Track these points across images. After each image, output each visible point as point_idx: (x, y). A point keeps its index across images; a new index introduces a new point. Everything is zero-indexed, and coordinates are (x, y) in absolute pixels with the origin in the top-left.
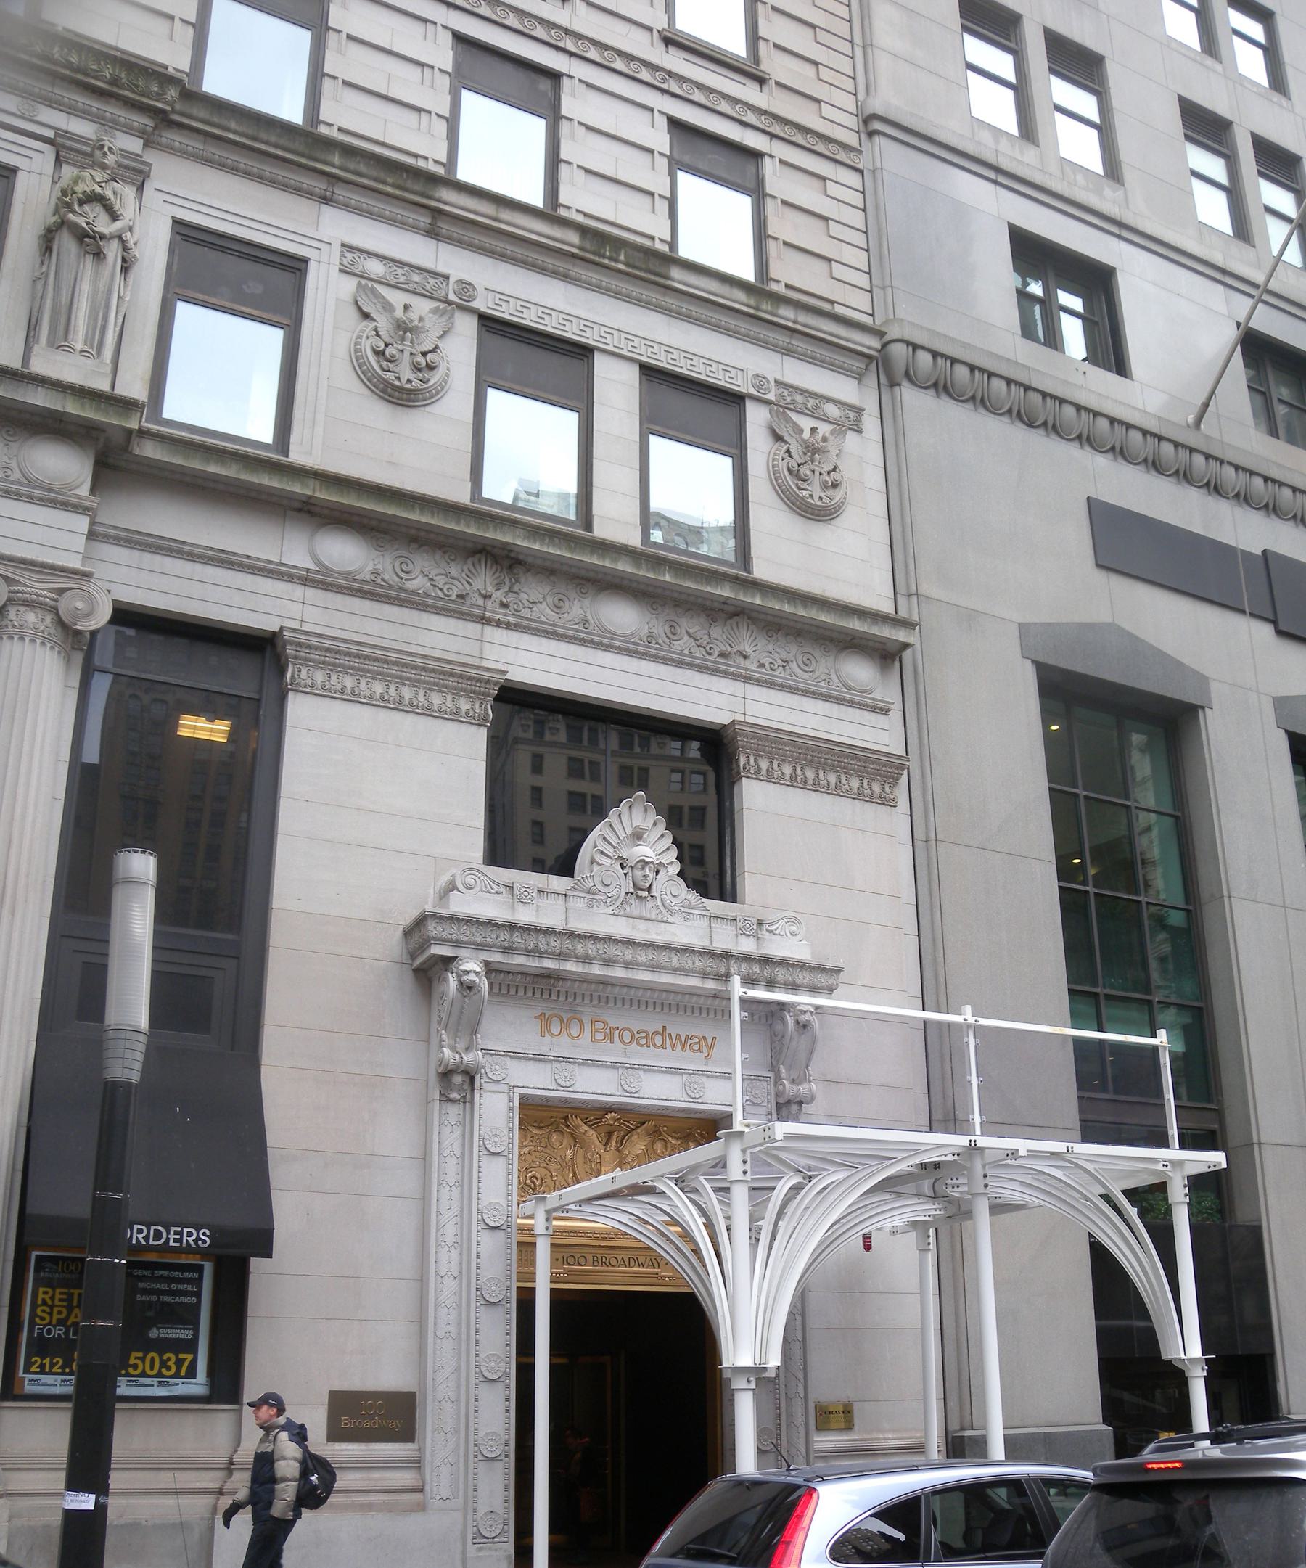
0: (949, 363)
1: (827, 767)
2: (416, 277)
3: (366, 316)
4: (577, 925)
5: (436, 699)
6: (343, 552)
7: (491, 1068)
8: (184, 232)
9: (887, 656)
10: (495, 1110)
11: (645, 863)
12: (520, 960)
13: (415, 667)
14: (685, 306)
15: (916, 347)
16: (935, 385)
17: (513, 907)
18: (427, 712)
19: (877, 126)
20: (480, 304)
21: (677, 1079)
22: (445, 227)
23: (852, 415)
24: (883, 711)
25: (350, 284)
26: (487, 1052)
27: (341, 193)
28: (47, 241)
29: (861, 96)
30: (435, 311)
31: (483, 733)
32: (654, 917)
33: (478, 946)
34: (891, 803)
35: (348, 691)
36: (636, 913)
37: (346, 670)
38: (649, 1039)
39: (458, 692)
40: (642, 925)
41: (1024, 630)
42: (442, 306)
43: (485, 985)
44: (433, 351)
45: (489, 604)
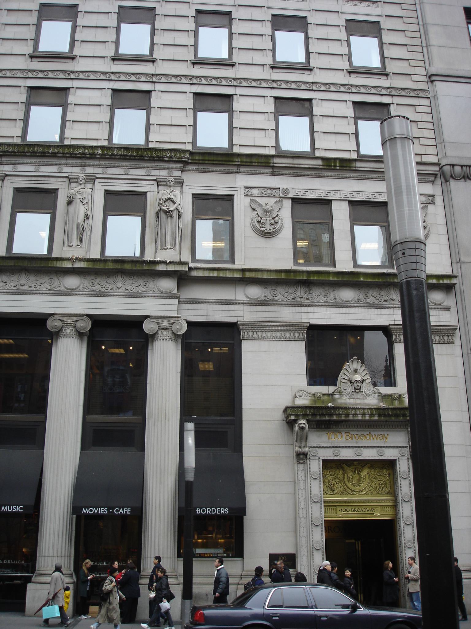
0: (468, 168)
2: (269, 191)
3: (254, 210)
5: (288, 335)
6: (255, 292)
8: (196, 197)
9: (449, 288)
11: (357, 381)
13: (280, 326)
15: (453, 166)
16: (464, 177)
18: (285, 339)
19: (434, 78)
20: (291, 195)
22: (276, 171)
23: (430, 198)
24: (448, 309)
25: (248, 199)
26: (310, 447)
27: (242, 169)
28: (157, 215)
29: (427, 67)
30: (276, 202)
31: (304, 343)
34: (452, 343)
35: (260, 337)
36: (355, 397)
37: (259, 330)
39: (295, 331)
42: (278, 199)
43: (307, 426)
44: (277, 216)
45: (302, 299)
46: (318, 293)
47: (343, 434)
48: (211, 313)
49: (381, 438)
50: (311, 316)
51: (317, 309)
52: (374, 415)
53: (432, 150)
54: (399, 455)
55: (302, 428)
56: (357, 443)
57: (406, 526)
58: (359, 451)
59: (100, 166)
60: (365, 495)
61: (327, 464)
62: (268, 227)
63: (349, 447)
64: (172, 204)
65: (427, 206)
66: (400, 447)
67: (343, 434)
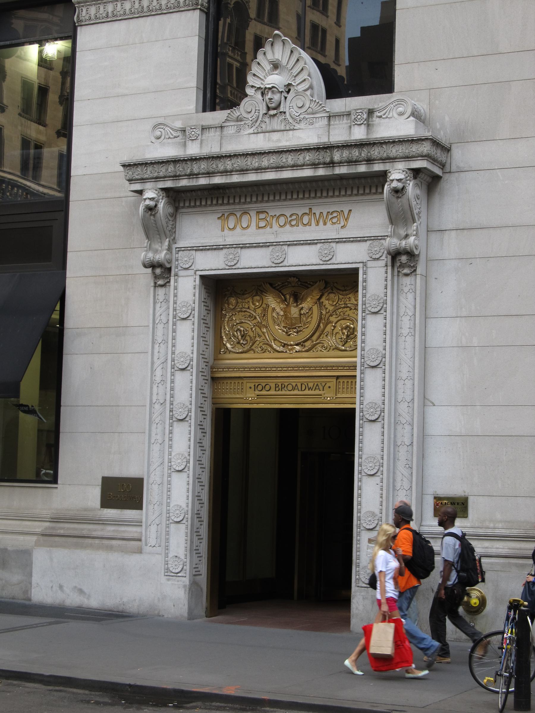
4: (230, 147)
7: (183, 258)
10: (187, 289)
17: (185, 145)
21: (313, 247)
32: (283, 128)
33: (157, 179)
36: (269, 128)
40: (275, 136)
47: (253, 214)
49: (334, 220)
56: (276, 234)
63: (258, 246)
67: (253, 214)
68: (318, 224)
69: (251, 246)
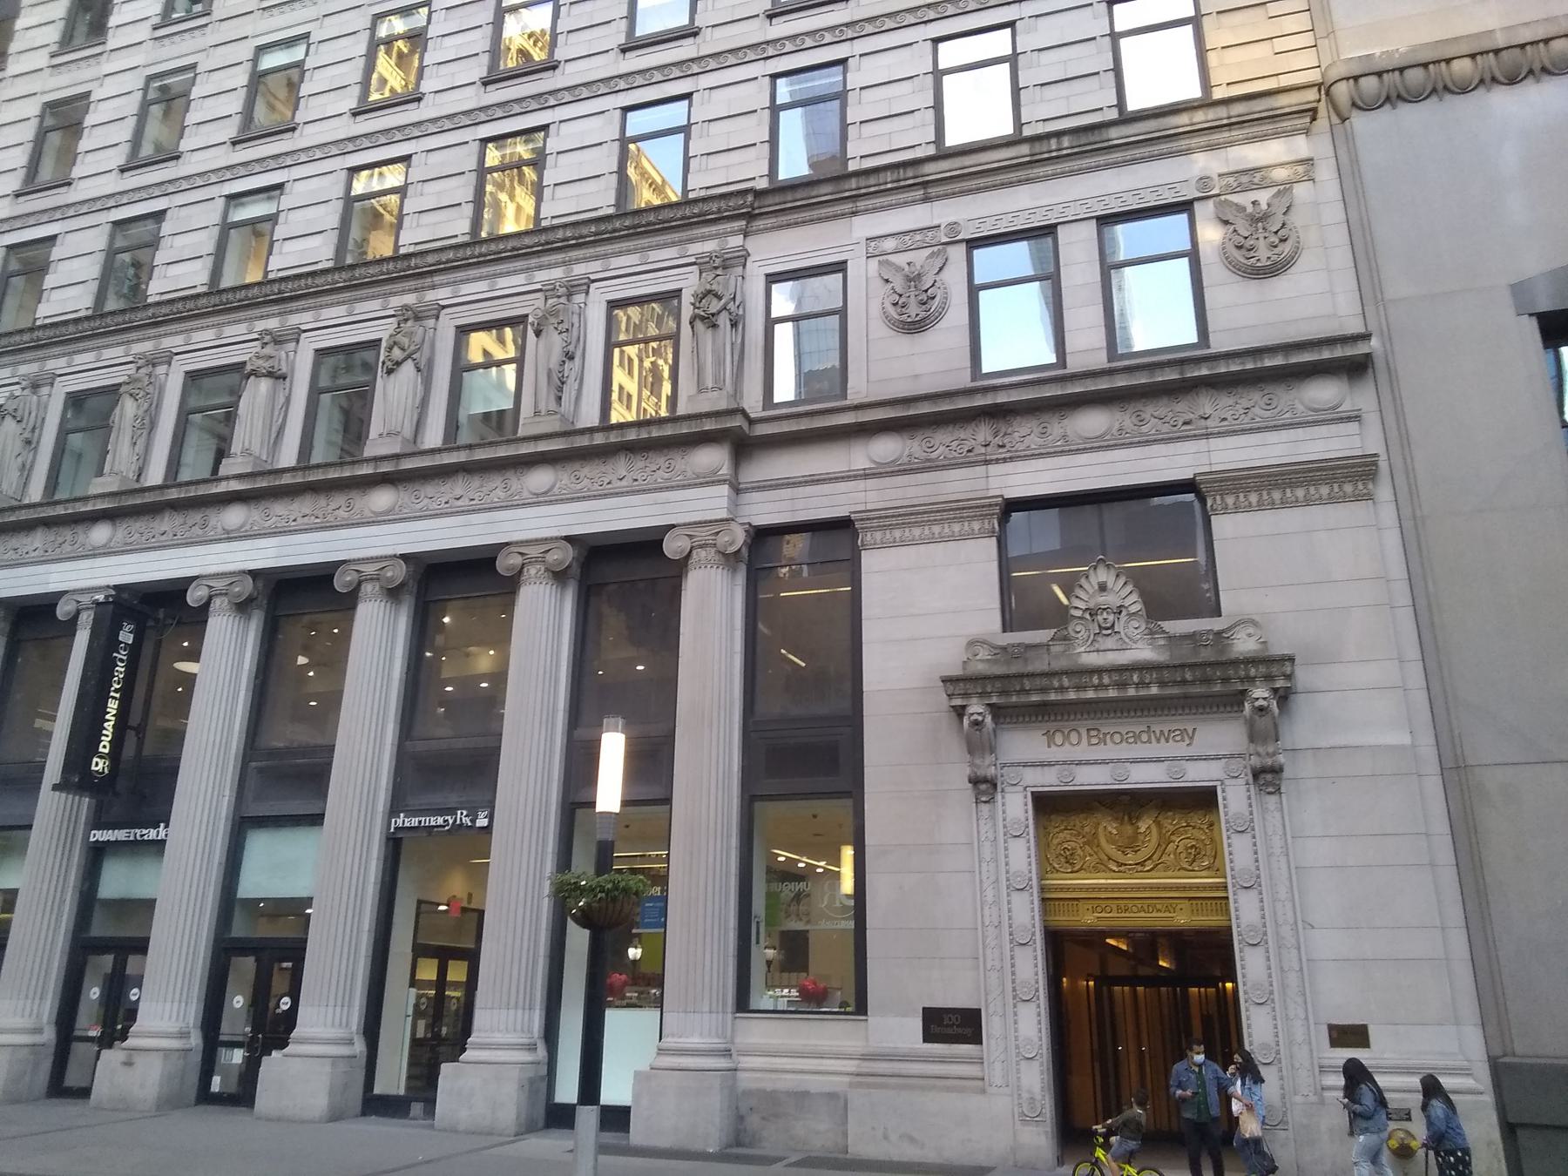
1: (1293, 485)
2: (918, 237)
5: (956, 527)
6: (886, 448)
9: (1356, 368)
12: (1014, 699)
14: (1129, 154)
15: (1356, 78)
22: (933, 191)
23: (1301, 169)
24: (1355, 418)
25: (874, 263)
26: (1004, 765)
27: (861, 204)
34: (1369, 497)
37: (891, 527)
38: (1137, 738)
39: (971, 518)
41: (1519, 291)
43: (989, 719)
45: (989, 449)
46: (1024, 430)
47: (1084, 732)
48: (800, 504)
50: (1012, 480)
51: (1020, 466)
52: (1148, 685)
53: (1308, 59)
54: (1222, 776)
55: (976, 723)
57: (1247, 949)
58: (1120, 769)
59: (597, 258)
60: (1152, 873)
61: (1048, 805)
62: (914, 311)
63: (1096, 762)
64: (715, 301)
65: (1291, 189)
66: (1224, 756)
68: (1158, 741)
69: (1088, 763)
